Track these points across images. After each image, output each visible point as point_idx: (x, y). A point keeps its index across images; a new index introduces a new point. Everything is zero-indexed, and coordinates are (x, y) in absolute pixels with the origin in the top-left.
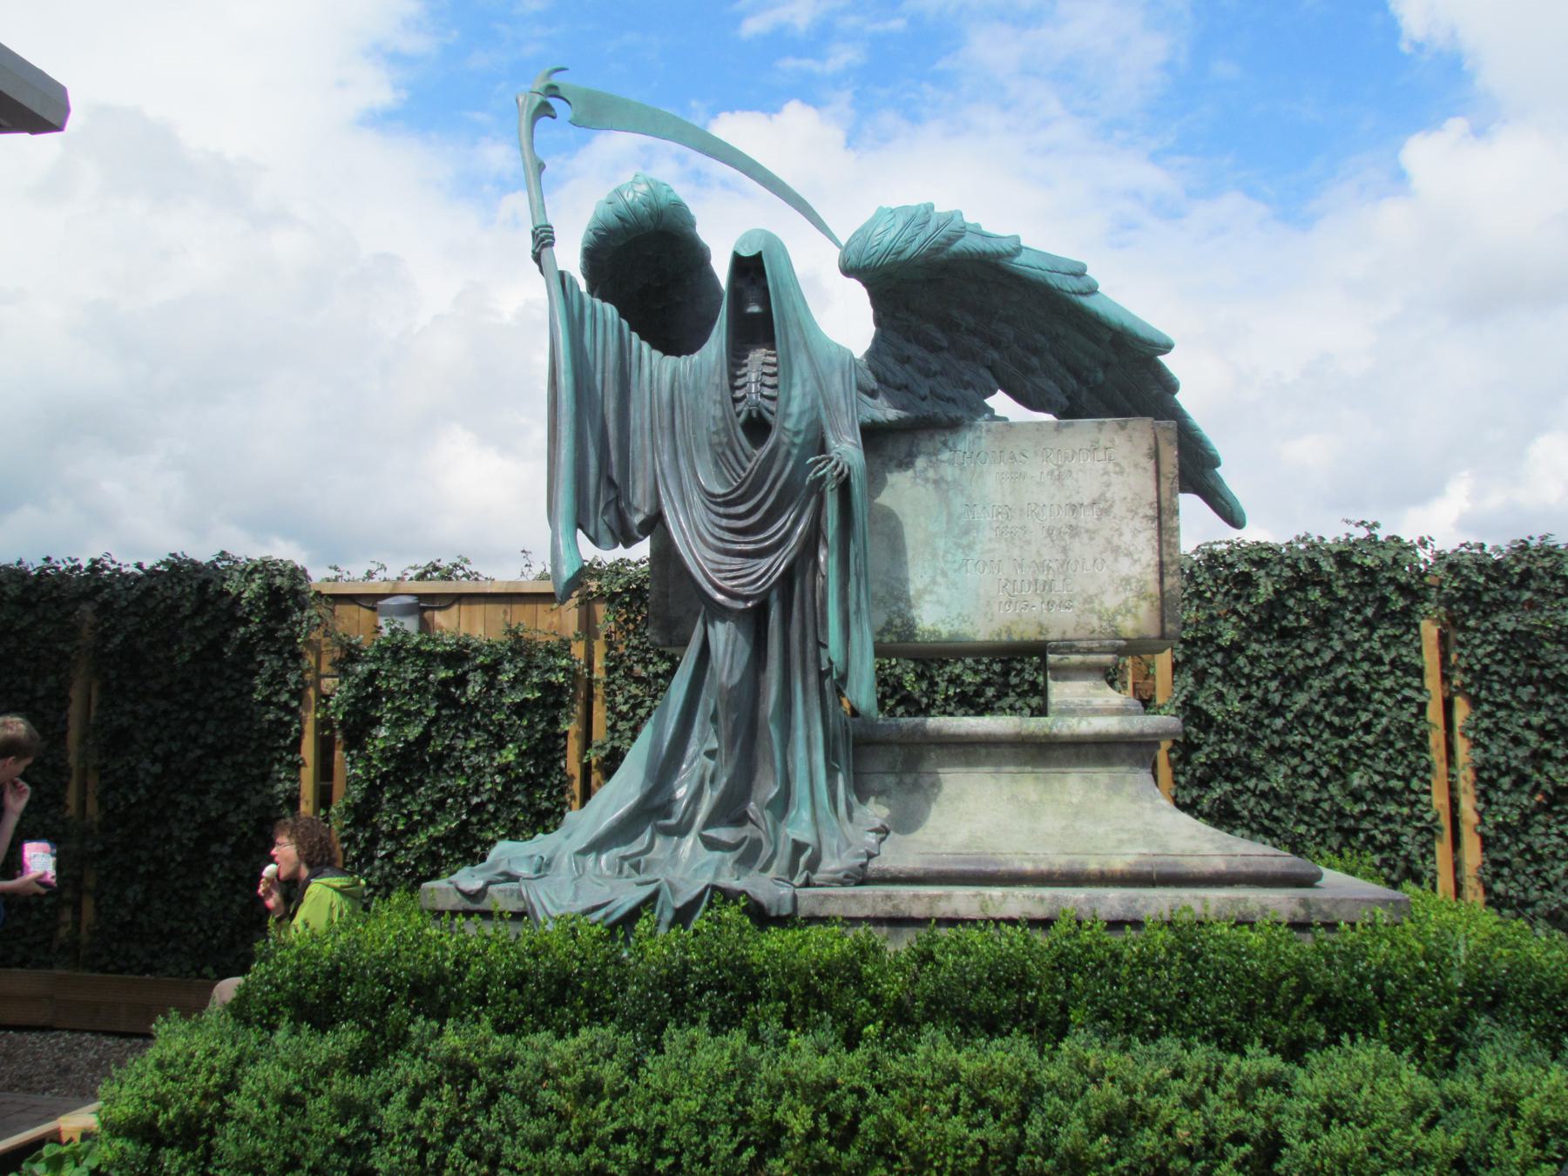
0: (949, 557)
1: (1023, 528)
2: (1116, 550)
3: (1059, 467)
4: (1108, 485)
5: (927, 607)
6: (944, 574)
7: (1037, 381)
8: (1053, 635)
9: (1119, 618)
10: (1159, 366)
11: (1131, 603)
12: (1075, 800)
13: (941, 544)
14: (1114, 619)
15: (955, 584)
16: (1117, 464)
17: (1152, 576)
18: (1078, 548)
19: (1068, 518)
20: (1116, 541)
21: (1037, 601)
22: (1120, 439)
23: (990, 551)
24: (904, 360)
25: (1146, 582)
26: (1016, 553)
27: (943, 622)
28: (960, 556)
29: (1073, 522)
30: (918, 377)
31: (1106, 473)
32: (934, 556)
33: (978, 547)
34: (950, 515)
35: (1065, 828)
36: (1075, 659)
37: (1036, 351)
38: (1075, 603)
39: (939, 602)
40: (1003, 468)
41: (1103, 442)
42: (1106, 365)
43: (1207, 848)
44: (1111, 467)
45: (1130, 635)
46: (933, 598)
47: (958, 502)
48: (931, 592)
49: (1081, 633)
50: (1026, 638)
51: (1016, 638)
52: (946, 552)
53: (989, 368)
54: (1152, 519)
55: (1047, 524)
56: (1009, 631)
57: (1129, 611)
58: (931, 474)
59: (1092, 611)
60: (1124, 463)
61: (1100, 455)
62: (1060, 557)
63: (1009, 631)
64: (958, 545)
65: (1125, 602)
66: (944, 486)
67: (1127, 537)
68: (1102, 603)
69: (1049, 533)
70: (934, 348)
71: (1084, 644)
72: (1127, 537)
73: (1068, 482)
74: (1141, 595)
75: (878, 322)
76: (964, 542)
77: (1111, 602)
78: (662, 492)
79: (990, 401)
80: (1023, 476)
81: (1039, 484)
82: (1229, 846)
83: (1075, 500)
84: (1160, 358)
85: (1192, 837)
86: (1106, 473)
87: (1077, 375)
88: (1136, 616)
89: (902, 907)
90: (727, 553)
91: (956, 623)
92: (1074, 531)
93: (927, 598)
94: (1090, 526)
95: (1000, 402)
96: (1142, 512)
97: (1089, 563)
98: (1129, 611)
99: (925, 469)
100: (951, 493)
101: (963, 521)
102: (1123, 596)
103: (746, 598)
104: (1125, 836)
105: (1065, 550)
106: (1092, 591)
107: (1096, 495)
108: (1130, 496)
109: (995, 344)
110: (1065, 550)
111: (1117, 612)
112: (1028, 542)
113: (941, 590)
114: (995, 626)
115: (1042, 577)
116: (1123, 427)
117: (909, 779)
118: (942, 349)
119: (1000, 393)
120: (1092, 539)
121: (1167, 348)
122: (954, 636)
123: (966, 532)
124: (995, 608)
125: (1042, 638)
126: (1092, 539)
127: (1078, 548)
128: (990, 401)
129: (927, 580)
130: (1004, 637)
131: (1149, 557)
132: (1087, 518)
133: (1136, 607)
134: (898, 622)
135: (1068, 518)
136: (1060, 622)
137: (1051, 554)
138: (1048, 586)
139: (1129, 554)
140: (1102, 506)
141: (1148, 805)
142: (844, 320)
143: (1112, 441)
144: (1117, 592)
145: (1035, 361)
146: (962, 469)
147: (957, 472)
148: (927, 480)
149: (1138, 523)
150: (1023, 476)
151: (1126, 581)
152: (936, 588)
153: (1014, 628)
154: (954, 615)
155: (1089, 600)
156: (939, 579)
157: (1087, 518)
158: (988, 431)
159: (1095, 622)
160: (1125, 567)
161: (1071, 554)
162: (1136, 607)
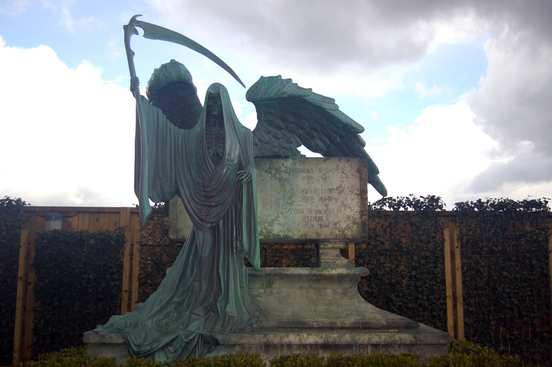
1: (312, 197)
2: (345, 206)
4: (343, 182)
5: (276, 225)
6: (282, 213)
7: (316, 141)
8: (322, 237)
9: (346, 231)
10: (359, 137)
12: (330, 299)
15: (286, 217)
16: (346, 174)
17: (358, 216)
20: (345, 202)
21: (316, 224)
24: (269, 133)
26: (309, 206)
27: (281, 231)
28: (288, 207)
30: (273, 139)
31: (342, 177)
33: (295, 204)
35: (327, 309)
36: (330, 246)
37: (315, 130)
38: (330, 225)
39: (280, 224)
40: (305, 174)
42: (340, 136)
43: (379, 317)
45: (350, 237)
46: (278, 222)
48: (277, 220)
49: (332, 237)
51: (308, 238)
52: (283, 205)
53: (299, 136)
55: (320, 196)
57: (349, 228)
58: (277, 176)
59: (336, 228)
60: (349, 174)
62: (325, 208)
65: (348, 225)
67: (349, 201)
69: (321, 199)
70: (279, 128)
72: (349, 201)
74: (354, 223)
75: (259, 118)
77: (343, 225)
78: (178, 180)
79: (299, 149)
80: (311, 178)
81: (318, 181)
82: (386, 316)
84: (360, 134)
85: (373, 313)
86: (342, 177)
87: (330, 139)
88: (352, 230)
89: (270, 340)
90: (204, 205)
92: (330, 199)
93: (276, 222)
94: (336, 197)
95: (303, 150)
96: (354, 192)
97: (336, 210)
99: (276, 174)
103: (212, 223)
104: (349, 312)
105: (326, 205)
106: (336, 221)
107: (338, 186)
109: (302, 128)
110: (326, 205)
111: (345, 229)
112: (313, 202)
113: (281, 220)
114: (301, 233)
115: (318, 215)
116: (348, 161)
117: (268, 291)
118: (282, 129)
120: (336, 201)
121: (362, 130)
122: (285, 237)
123: (291, 198)
125: (318, 238)
126: (336, 201)
127: (332, 206)
128: (299, 149)
130: (304, 237)
132: (335, 195)
134: (264, 231)
136: (325, 233)
137: (321, 207)
138: (320, 219)
139: (350, 208)
141: (356, 300)
142: (247, 116)
143: (344, 165)
144: (345, 221)
145: (315, 134)
147: (287, 175)
148: (276, 178)
149: (353, 196)
151: (349, 217)
152: (279, 219)
153: (307, 234)
154: (286, 229)
155: (335, 224)
156: (280, 215)
159: (337, 232)
160: (348, 212)
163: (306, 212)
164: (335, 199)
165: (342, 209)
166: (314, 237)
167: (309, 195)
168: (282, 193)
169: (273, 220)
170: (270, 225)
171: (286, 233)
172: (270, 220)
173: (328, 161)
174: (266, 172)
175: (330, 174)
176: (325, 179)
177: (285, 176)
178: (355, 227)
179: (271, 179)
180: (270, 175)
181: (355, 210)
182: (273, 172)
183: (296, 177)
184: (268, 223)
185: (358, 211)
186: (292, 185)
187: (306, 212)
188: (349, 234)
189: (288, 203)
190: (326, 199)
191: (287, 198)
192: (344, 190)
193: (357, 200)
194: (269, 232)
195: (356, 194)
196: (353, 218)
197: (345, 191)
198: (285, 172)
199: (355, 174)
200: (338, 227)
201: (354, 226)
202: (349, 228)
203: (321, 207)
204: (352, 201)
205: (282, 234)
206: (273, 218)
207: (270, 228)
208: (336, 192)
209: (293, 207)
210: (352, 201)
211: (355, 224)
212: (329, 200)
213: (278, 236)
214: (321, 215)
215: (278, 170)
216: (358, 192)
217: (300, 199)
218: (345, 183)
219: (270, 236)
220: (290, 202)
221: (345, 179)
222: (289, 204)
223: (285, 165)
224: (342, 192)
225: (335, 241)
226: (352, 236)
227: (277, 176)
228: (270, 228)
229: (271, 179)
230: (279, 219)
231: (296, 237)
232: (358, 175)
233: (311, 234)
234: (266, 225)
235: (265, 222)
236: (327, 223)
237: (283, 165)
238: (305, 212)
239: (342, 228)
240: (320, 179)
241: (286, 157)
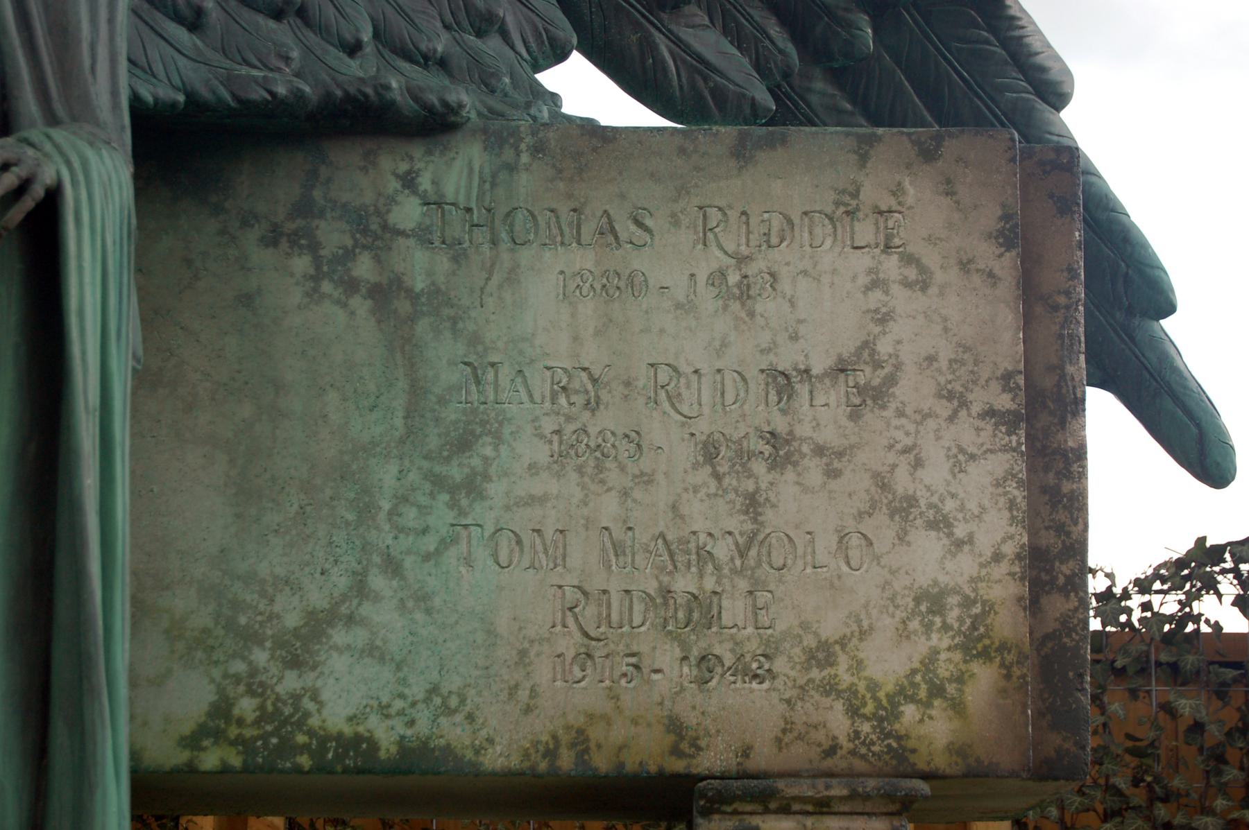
0: (410, 516)
1: (635, 439)
2: (903, 509)
3: (742, 260)
5: (339, 663)
6: (393, 567)
7: (686, 34)
9: (910, 712)
11: (944, 670)
13: (387, 475)
14: (897, 716)
15: (423, 598)
16: (909, 259)
17: (1004, 588)
18: (797, 502)
19: (761, 412)
20: (902, 482)
21: (666, 656)
22: (918, 191)
23: (533, 500)
25: (989, 608)
26: (609, 508)
27: (384, 711)
28: (442, 516)
29: (780, 424)
31: (877, 283)
32: (366, 511)
33: (496, 489)
34: (417, 391)
38: (780, 665)
39: (373, 651)
40: (583, 260)
41: (872, 193)
44: (891, 266)
45: (941, 763)
46: (359, 637)
47: (443, 358)
48: (350, 620)
49: (799, 755)
50: (631, 766)
51: (602, 763)
52: (403, 499)
54: (1009, 421)
55: (703, 427)
56: (580, 740)
59: (830, 688)
60: (931, 258)
61: (865, 231)
62: (738, 524)
63: (580, 740)
64: (438, 482)
66: (403, 306)
67: (936, 473)
68: (858, 665)
69: (709, 452)
71: (804, 789)
72: (936, 473)
73: (767, 306)
74: (975, 644)
76: (456, 472)
77: (887, 662)
79: (549, 79)
80: (634, 284)
81: (686, 307)
83: (786, 359)
86: (877, 283)
88: (957, 707)
91: (423, 717)
92: (780, 450)
94: (829, 436)
95: (583, 88)
96: (980, 399)
97: (826, 543)
98: (937, 691)
99: (349, 255)
100: (422, 327)
101: (452, 413)
102: (921, 647)
105: (753, 505)
106: (831, 628)
107: (847, 347)
108: (946, 353)
110: (753, 505)
111: (904, 693)
112: (645, 479)
113: (384, 616)
114: (540, 727)
115: (684, 584)
116: (928, 154)
119: (576, 58)
123: (464, 444)
124: (543, 673)
125: (678, 766)
127: (797, 502)
128: (549, 79)
129: (341, 582)
130: (566, 761)
131: (997, 530)
132: (822, 416)
133: (960, 679)
134: (246, 707)
135: (761, 412)
137: (711, 517)
138: (703, 611)
139: (940, 523)
140: (864, 380)
144: (903, 634)
146: (458, 258)
147: (443, 263)
148: (352, 286)
149: (967, 432)
150: (634, 284)
151: (932, 601)
152: (366, 609)
153: (596, 733)
154: (417, 690)
155: (822, 655)
156: (378, 581)
157: (822, 416)
158: (538, 149)
159: (838, 722)
160: (926, 560)
161: (769, 515)
162: (960, 679)
163: (583, 554)
164: (820, 451)
165: (883, 529)
166: (647, 752)
167: (609, 420)
168: (399, 404)
169: (317, 625)
170: (295, 663)
171: (423, 726)
172: (292, 620)
173: (761, 156)
174: (272, 239)
175: (784, 257)
176: (745, 293)
177: (419, 266)
178: (984, 676)
179: (314, 295)
180: (302, 264)
181: (985, 544)
182: (333, 235)
183: (512, 277)
184: (279, 644)
185: (1009, 549)
186: (475, 340)
187: (583, 554)
188: (933, 732)
189: (438, 482)
190: (744, 456)
191: (433, 442)
192: (891, 380)
193: (999, 464)
194: (283, 718)
195: (990, 413)
196: (967, 603)
197: (903, 391)
198: (423, 236)
199: (987, 254)
200: (846, 679)
201: (976, 667)
202: (937, 691)
203: (711, 517)
204: (958, 469)
205: (387, 736)
206: (318, 599)
207: (291, 682)
208: (832, 398)
209: (486, 514)
210: (958, 469)
211: (985, 655)
212: (776, 464)
213: (361, 744)
214: (709, 584)
215: (373, 231)
216: (1005, 402)
217: (541, 453)
218: (898, 329)
219: (287, 748)
220: (456, 472)
221: (900, 299)
222: (453, 490)
223: (425, 183)
224: (877, 395)
225: (818, 789)
226: (958, 750)
227: (364, 268)
228: (291, 682)
229: (314, 295)
230: (366, 609)
231: (496, 759)
232: (1006, 265)
233: (619, 732)
234: (260, 657)
235: (251, 637)
236: (753, 646)
237: (409, 182)
238: (575, 560)
239: (873, 686)
240: (707, 300)
241: (436, 125)
